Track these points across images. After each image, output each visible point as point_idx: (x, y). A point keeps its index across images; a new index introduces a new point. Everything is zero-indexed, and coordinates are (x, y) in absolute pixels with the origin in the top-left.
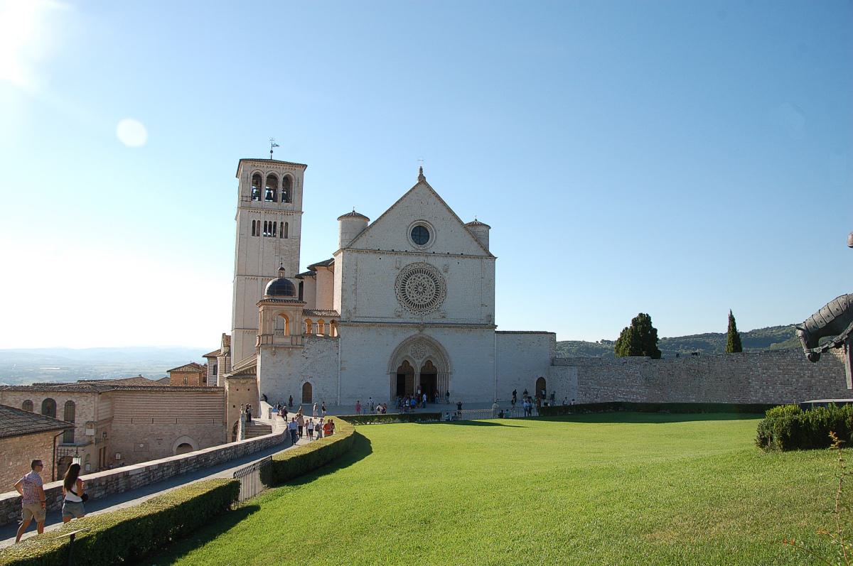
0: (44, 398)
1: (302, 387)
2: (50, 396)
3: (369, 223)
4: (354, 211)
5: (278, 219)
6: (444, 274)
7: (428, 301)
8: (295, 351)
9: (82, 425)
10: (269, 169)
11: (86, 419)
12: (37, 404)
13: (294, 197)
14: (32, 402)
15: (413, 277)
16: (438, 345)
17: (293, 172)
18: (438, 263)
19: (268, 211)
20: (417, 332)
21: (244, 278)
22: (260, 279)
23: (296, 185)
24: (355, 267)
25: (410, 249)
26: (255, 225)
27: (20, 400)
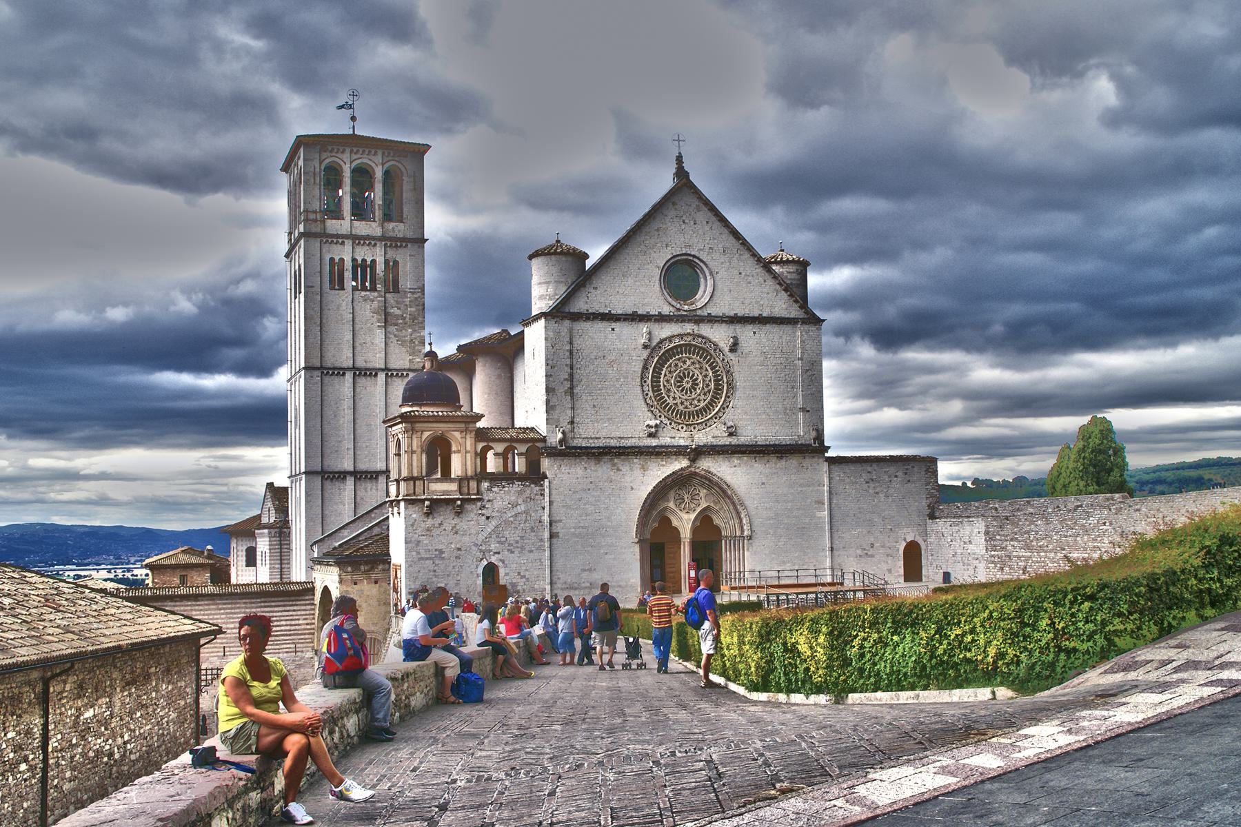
1: (480, 570)
3: (589, 263)
4: (558, 241)
7: (702, 404)
8: (468, 507)
10: (359, 156)
16: (725, 487)
18: (720, 335)
19: (357, 240)
20: (683, 463)
22: (349, 376)
24: (568, 348)
25: (666, 310)
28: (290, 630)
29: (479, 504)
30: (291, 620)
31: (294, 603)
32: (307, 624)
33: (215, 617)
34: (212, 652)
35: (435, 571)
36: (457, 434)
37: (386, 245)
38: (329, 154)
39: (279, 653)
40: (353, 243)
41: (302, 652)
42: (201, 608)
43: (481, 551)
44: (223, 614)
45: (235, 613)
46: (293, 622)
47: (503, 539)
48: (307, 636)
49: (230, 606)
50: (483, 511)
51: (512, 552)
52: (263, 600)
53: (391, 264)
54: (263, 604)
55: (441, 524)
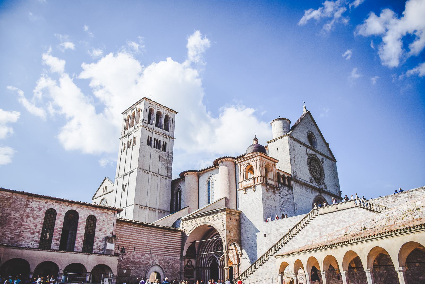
0: (69, 208)
2: (74, 207)
5: (162, 139)
6: (323, 165)
7: (319, 177)
8: (277, 192)
9: (101, 240)
11: (106, 234)
12: (60, 214)
13: (171, 128)
14: (55, 211)
15: (312, 162)
17: (170, 114)
19: (156, 133)
21: (141, 170)
22: (150, 173)
23: (172, 122)
26: (149, 140)
27: (44, 207)
28: (173, 247)
29: (279, 192)
30: (174, 243)
31: (175, 236)
32: (179, 245)
33: (149, 236)
34: (146, 251)
35: (270, 213)
36: (272, 165)
37: (164, 136)
38: (151, 106)
39: (169, 256)
40: (155, 133)
41: (177, 257)
42: (144, 231)
43: (281, 209)
44: (151, 235)
45: (156, 236)
46: (175, 244)
47: (285, 206)
48: (179, 250)
49: (154, 232)
50: (280, 195)
51: (288, 212)
52: (165, 232)
53: (165, 143)
54: (165, 234)
55: (271, 196)
